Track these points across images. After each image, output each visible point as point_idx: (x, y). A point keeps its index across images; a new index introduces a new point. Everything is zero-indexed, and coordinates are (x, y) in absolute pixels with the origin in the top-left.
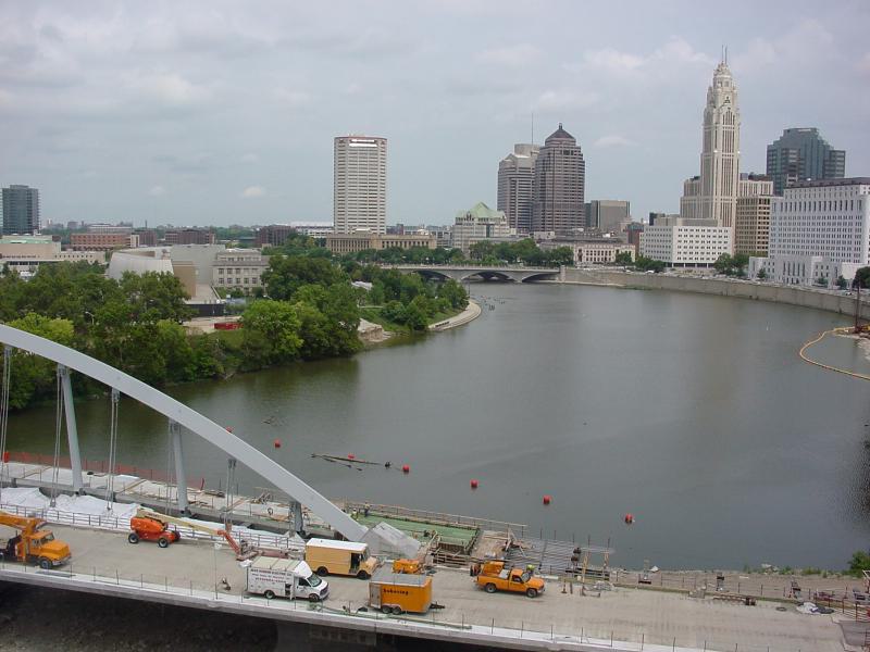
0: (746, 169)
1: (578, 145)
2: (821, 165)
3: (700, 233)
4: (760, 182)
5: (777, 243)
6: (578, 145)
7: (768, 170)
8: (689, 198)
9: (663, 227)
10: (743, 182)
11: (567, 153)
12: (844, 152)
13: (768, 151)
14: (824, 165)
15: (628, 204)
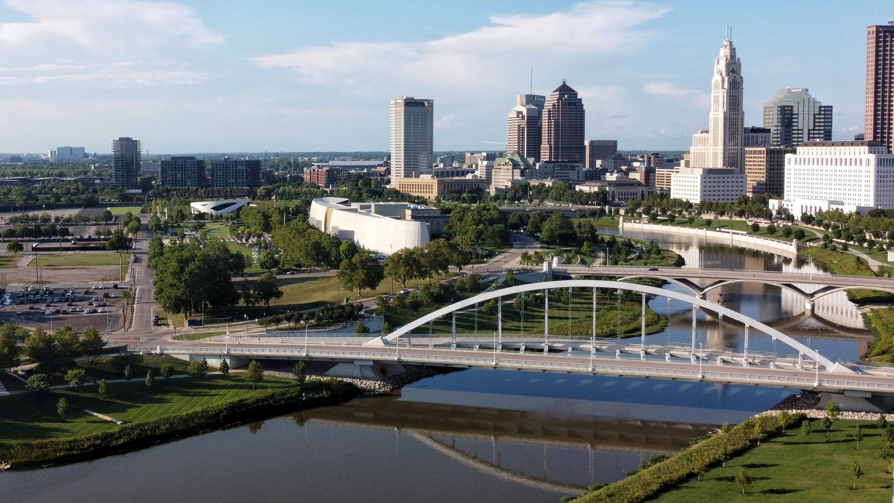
0: (749, 123)
1: (579, 97)
2: (812, 118)
3: (717, 180)
4: (760, 134)
5: (792, 189)
6: (579, 97)
7: (765, 123)
8: (703, 147)
9: (690, 176)
10: (747, 134)
11: (570, 104)
12: (831, 107)
13: (765, 108)
14: (815, 118)
15: (616, 142)
